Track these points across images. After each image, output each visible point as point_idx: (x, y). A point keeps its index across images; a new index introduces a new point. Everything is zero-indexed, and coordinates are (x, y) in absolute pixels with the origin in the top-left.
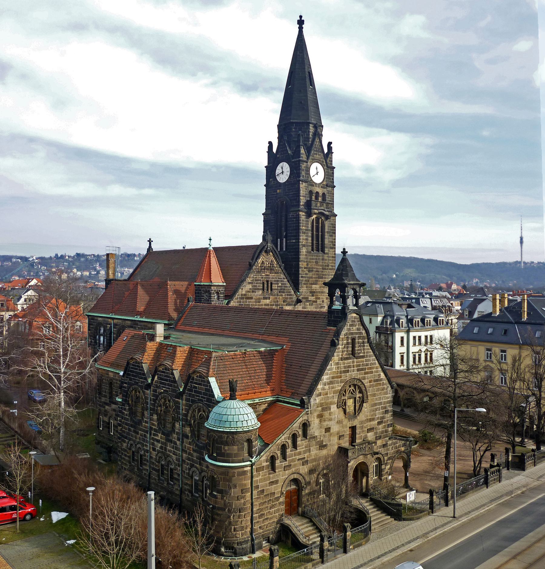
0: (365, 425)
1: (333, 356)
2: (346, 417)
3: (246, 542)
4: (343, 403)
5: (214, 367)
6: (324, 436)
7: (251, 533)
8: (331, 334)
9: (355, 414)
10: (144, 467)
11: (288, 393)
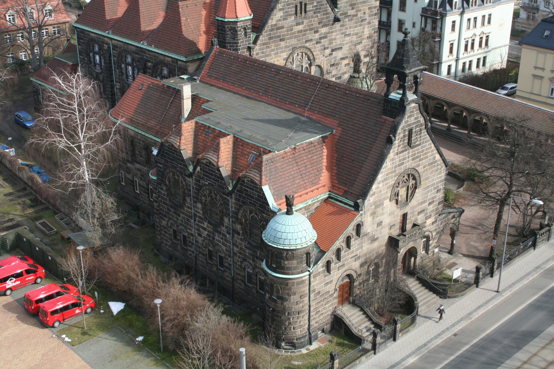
0: (416, 209)
1: (389, 153)
2: (398, 207)
3: (304, 337)
4: (395, 195)
5: (266, 173)
6: (376, 230)
7: (309, 329)
8: (386, 125)
9: (407, 201)
10: (189, 248)
11: (340, 190)
